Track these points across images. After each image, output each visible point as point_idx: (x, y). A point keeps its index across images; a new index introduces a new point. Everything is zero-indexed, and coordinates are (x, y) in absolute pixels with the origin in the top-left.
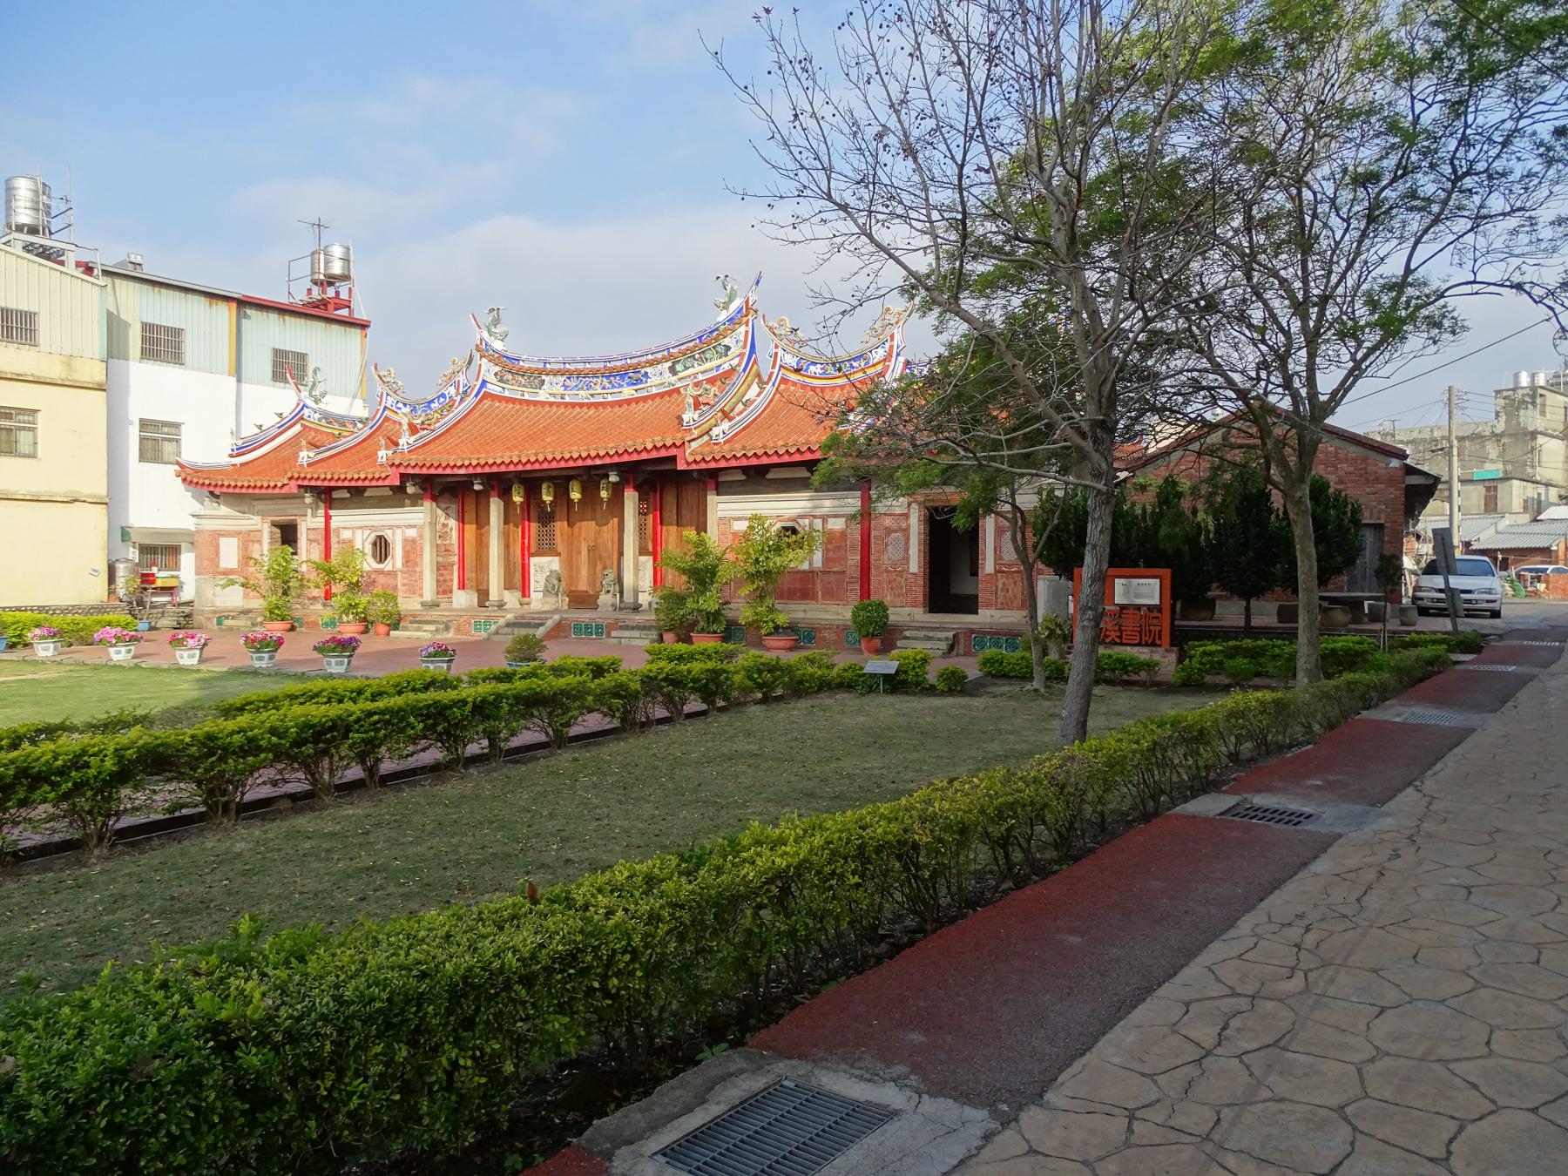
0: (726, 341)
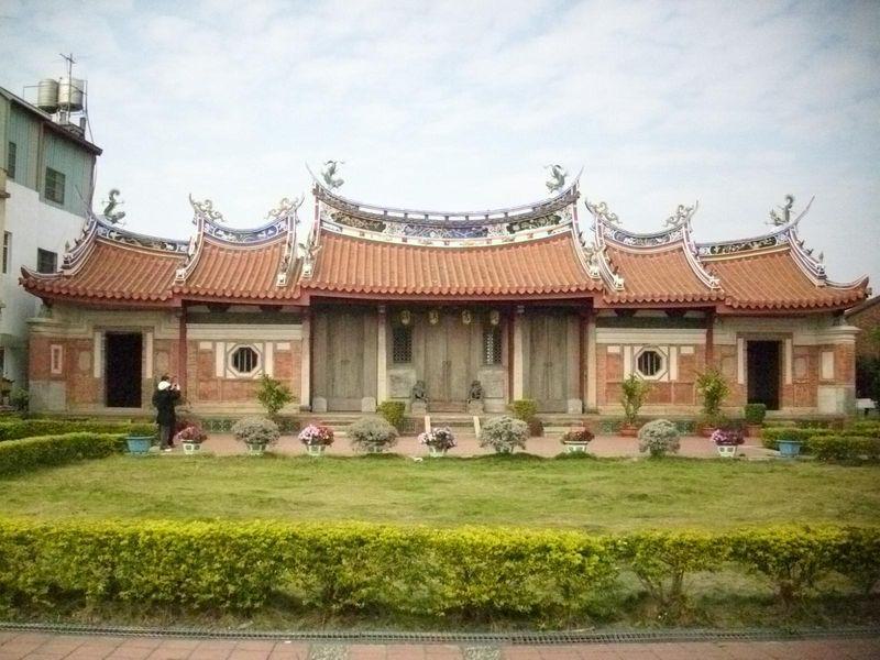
0: (558, 213)
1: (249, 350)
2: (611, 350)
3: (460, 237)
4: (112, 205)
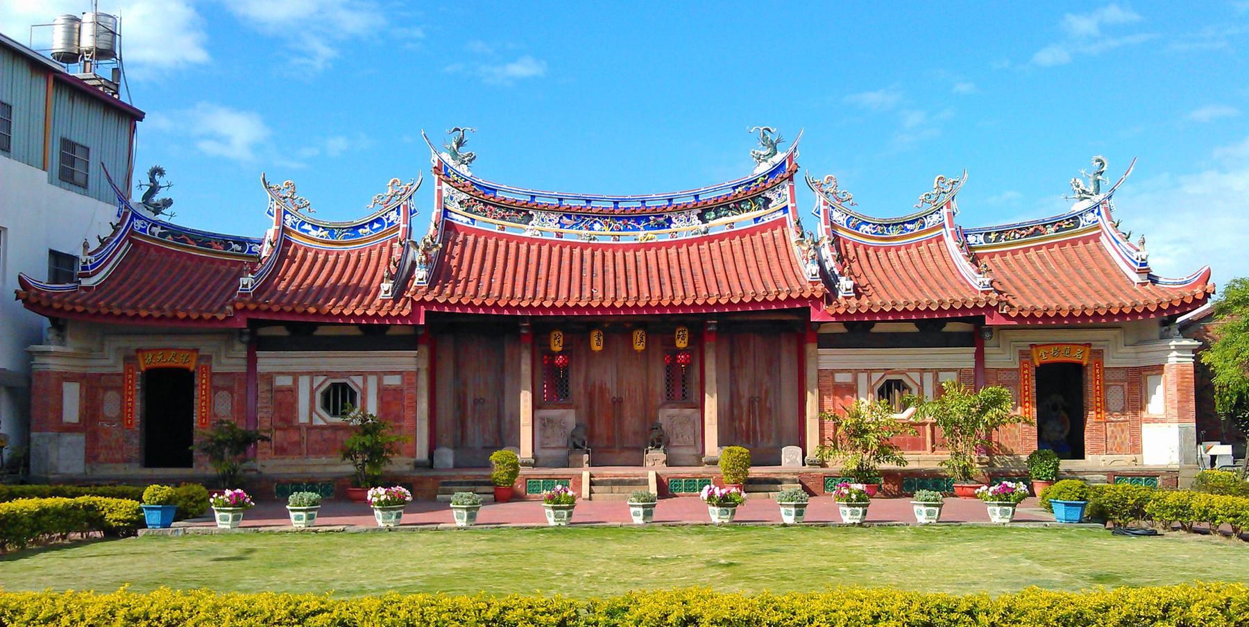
0: (768, 195)
1: (345, 386)
2: (840, 378)
3: (635, 229)
4: (154, 189)
